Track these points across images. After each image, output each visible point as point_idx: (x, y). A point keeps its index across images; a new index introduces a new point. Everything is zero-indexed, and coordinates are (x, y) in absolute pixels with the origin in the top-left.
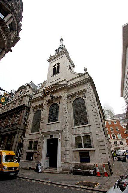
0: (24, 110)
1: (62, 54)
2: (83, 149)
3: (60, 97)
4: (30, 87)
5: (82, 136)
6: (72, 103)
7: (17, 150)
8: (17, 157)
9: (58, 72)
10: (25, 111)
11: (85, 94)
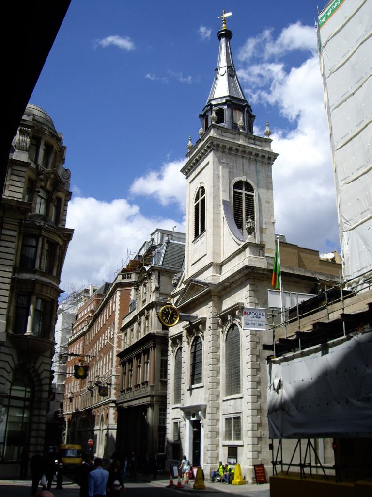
1: (206, 151)
2: (233, 442)
3: (203, 322)
5: (232, 419)
9: (203, 230)
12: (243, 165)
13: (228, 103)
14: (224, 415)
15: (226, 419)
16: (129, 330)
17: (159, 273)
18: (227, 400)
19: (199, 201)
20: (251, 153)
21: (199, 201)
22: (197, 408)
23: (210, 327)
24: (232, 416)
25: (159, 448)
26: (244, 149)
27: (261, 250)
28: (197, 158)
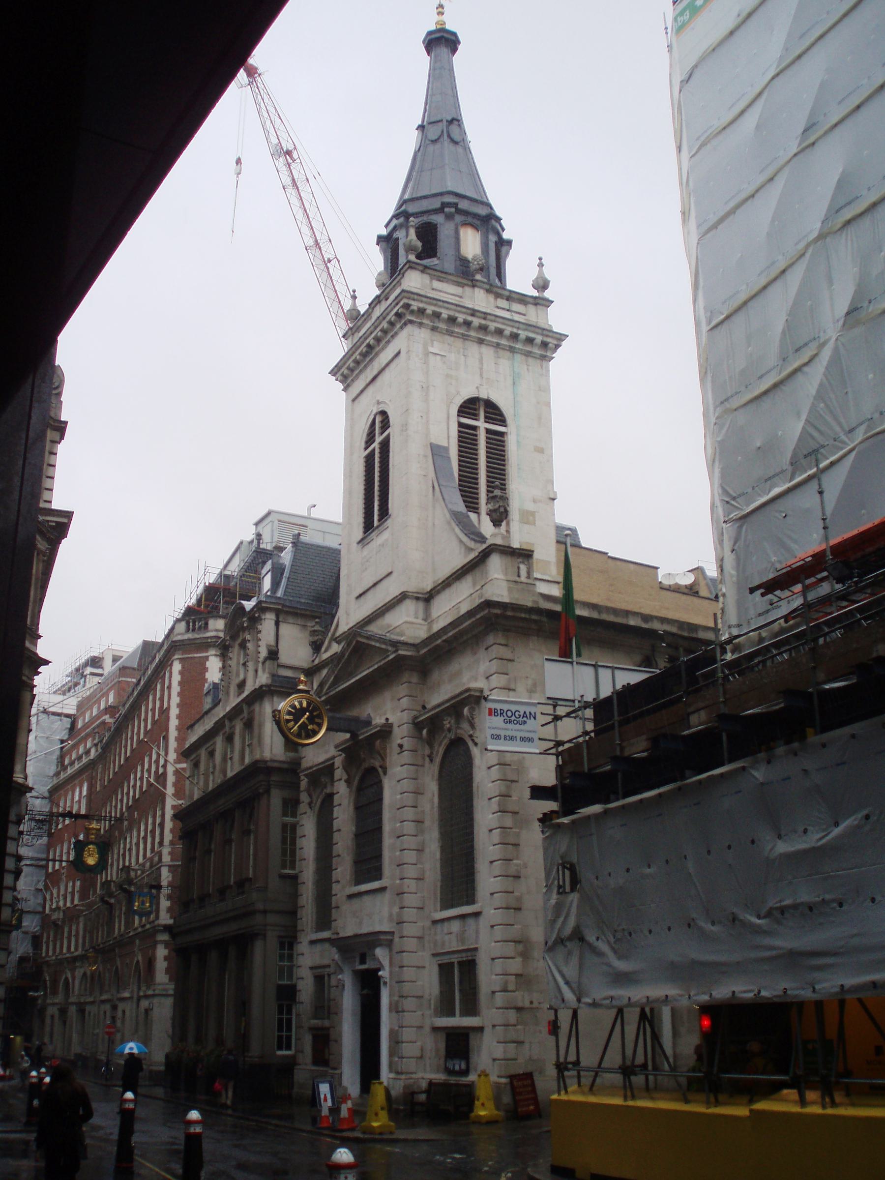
0: (268, 791)
1: (392, 324)
3: (386, 732)
4: (278, 613)
5: (456, 965)
6: (435, 768)
7: (280, 1021)
8: (289, 1047)
9: (384, 512)
10: (276, 799)
11: (472, 726)
12: (481, 361)
13: (446, 210)
14: (434, 955)
15: (440, 965)
16: (203, 753)
17: (277, 616)
18: (443, 921)
19: (376, 445)
20: (499, 332)
21: (376, 445)
22: (373, 940)
23: (401, 746)
24: (455, 959)
25: (280, 1038)
26: (483, 322)
27: (523, 563)
28: (370, 340)
